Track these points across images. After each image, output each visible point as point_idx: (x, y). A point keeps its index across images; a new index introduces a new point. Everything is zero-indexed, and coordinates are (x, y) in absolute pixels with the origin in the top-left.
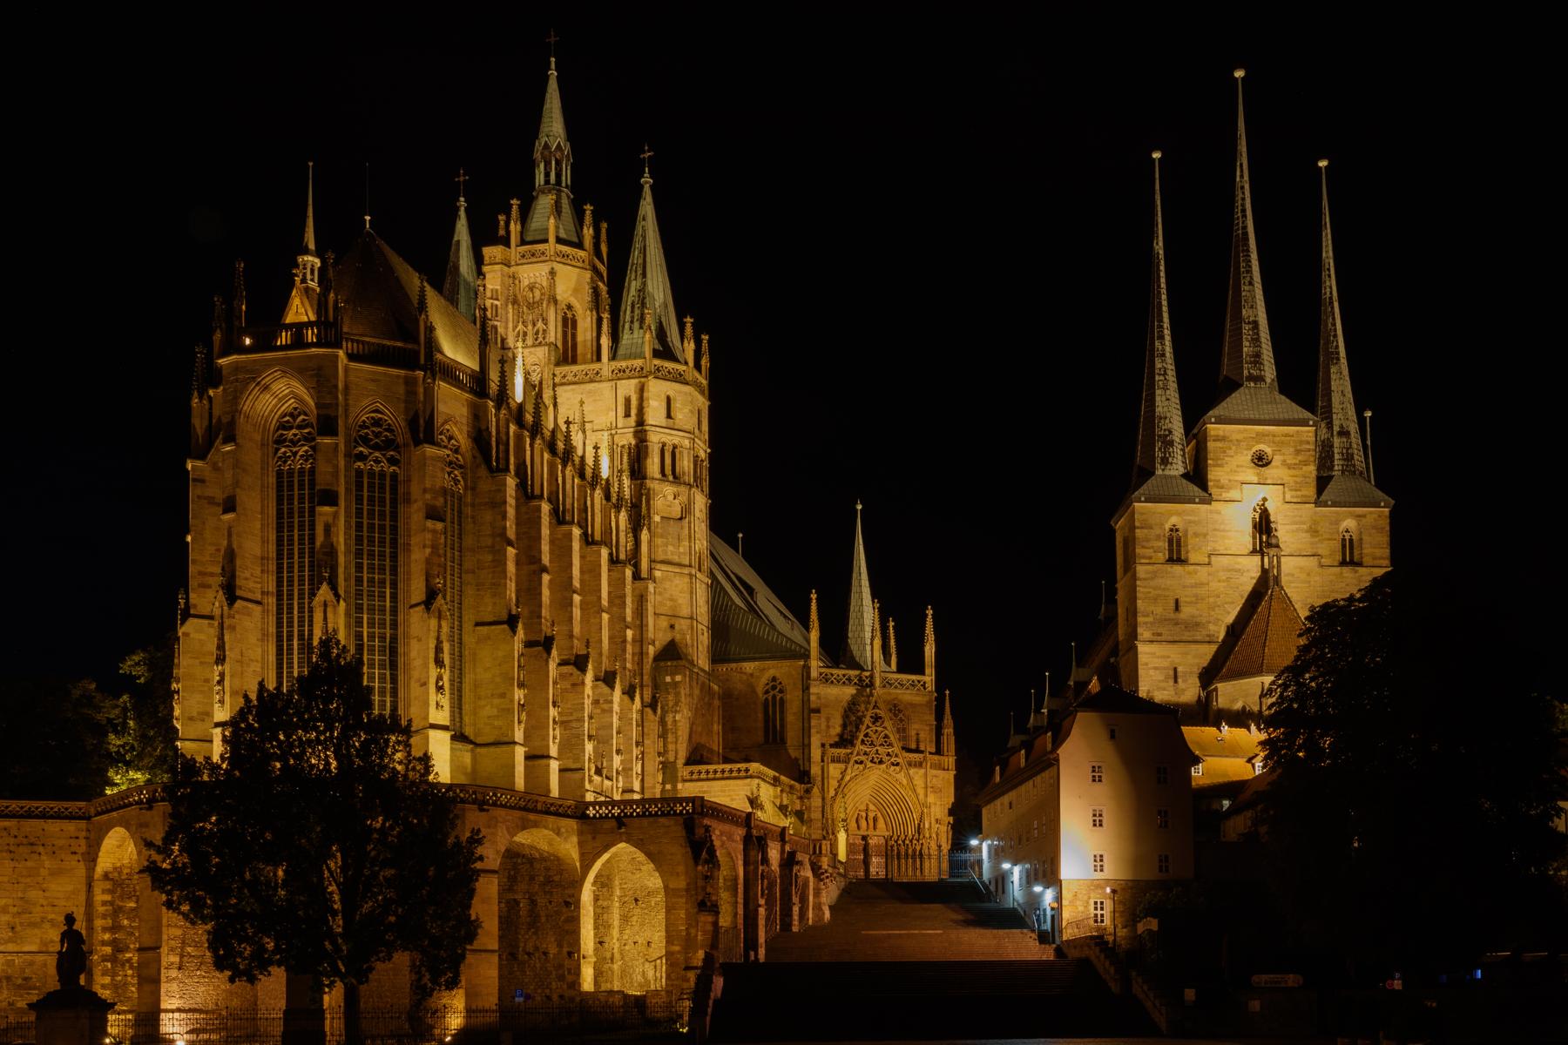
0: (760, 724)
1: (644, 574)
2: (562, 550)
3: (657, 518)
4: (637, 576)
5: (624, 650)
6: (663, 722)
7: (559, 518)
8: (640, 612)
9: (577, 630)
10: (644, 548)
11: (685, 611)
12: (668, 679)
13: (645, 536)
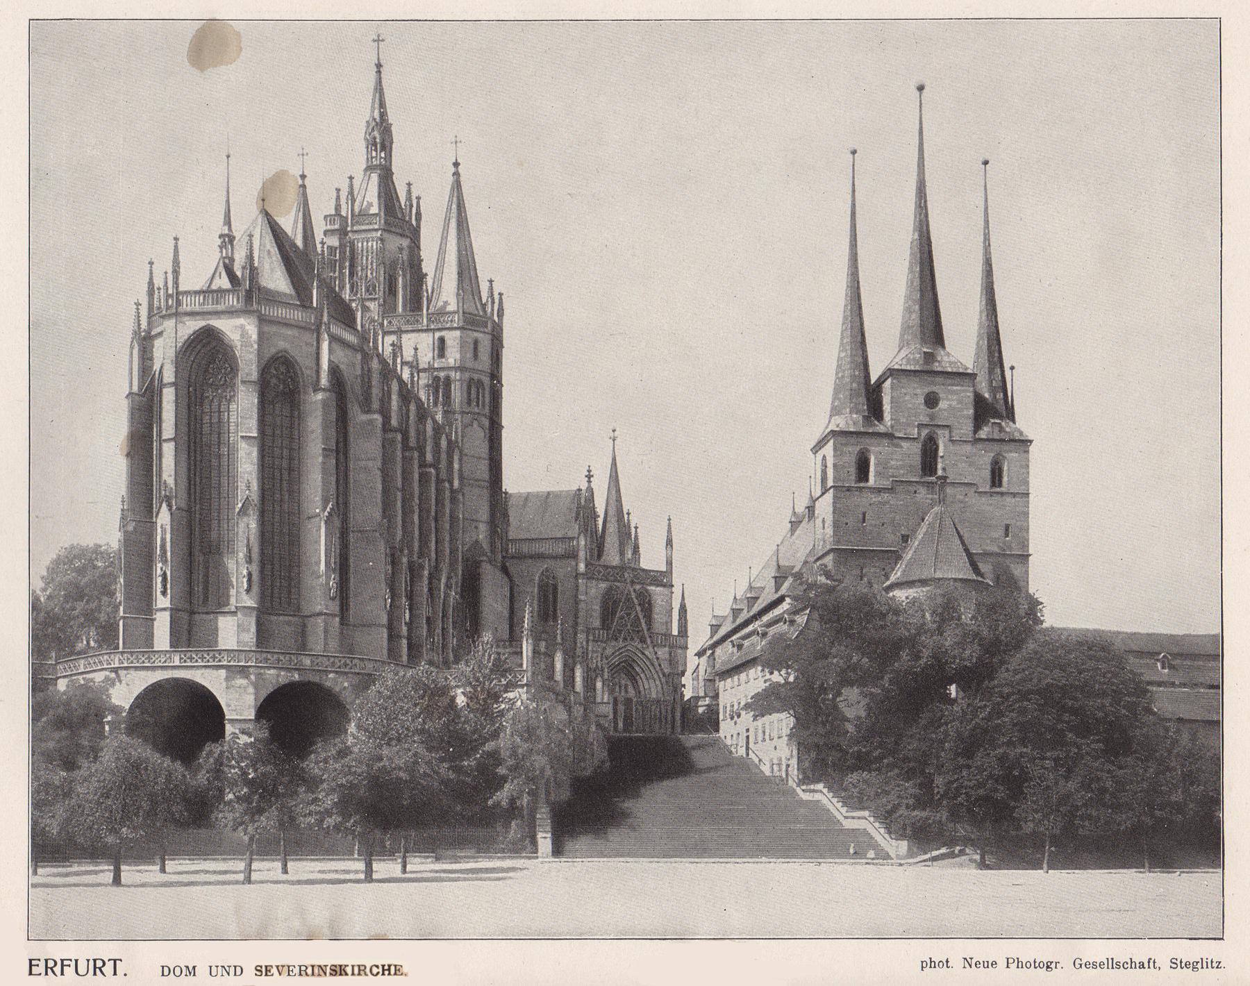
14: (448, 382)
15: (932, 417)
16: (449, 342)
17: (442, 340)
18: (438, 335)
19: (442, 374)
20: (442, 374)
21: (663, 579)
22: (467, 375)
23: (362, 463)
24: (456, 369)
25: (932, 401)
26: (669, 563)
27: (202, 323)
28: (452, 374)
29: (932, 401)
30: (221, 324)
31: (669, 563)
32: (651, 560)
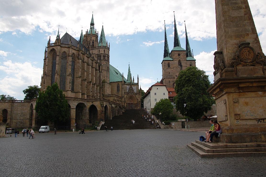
0: (116, 89)
1: (101, 71)
2: (88, 69)
3: (102, 64)
4: (100, 72)
5: (97, 81)
6: (103, 89)
7: (88, 65)
8: (100, 76)
9: (90, 78)
10: (101, 68)
11: (106, 76)
12: (103, 84)
13: (101, 67)
14: (100, 56)
15: (179, 57)
16: (100, 51)
17: (99, 50)
18: (99, 49)
19: (99, 55)
20: (99, 55)
21: (137, 84)
22: (103, 55)
23: (78, 67)
24: (102, 54)
25: (179, 55)
26: (138, 81)
27: (51, 48)
28: (101, 55)
29: (179, 55)
30: (54, 48)
31: (138, 81)
32: (136, 81)
